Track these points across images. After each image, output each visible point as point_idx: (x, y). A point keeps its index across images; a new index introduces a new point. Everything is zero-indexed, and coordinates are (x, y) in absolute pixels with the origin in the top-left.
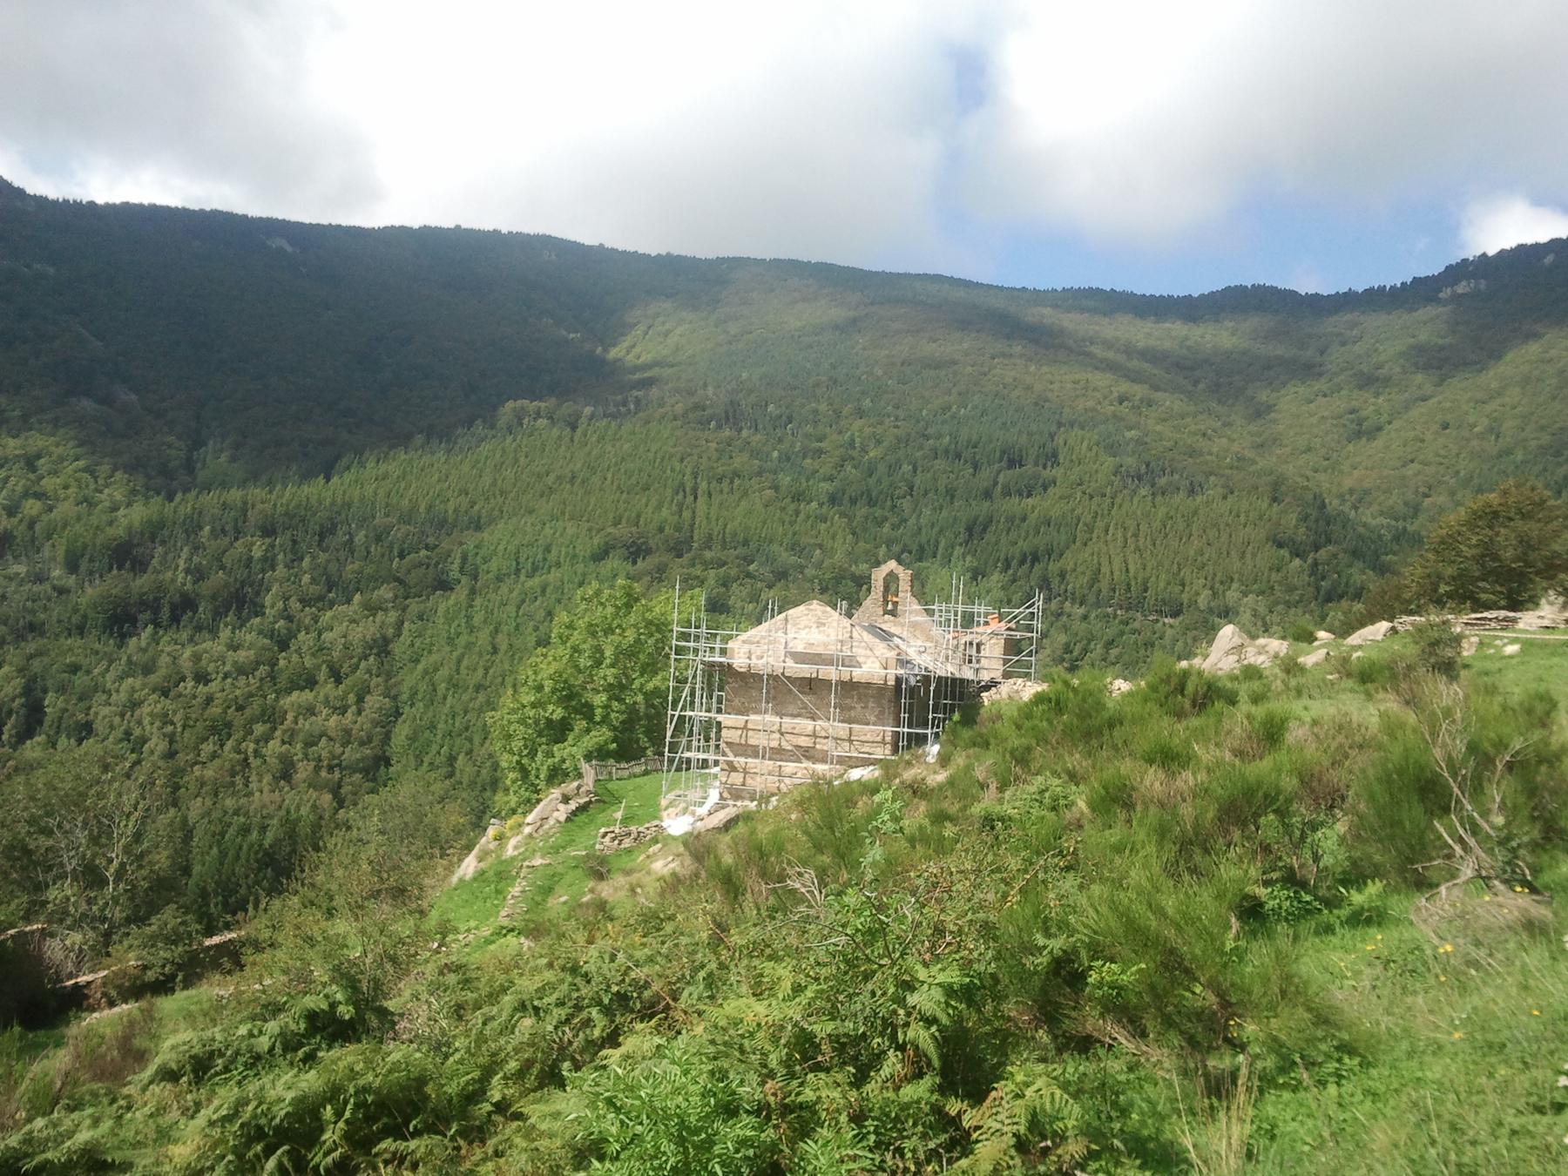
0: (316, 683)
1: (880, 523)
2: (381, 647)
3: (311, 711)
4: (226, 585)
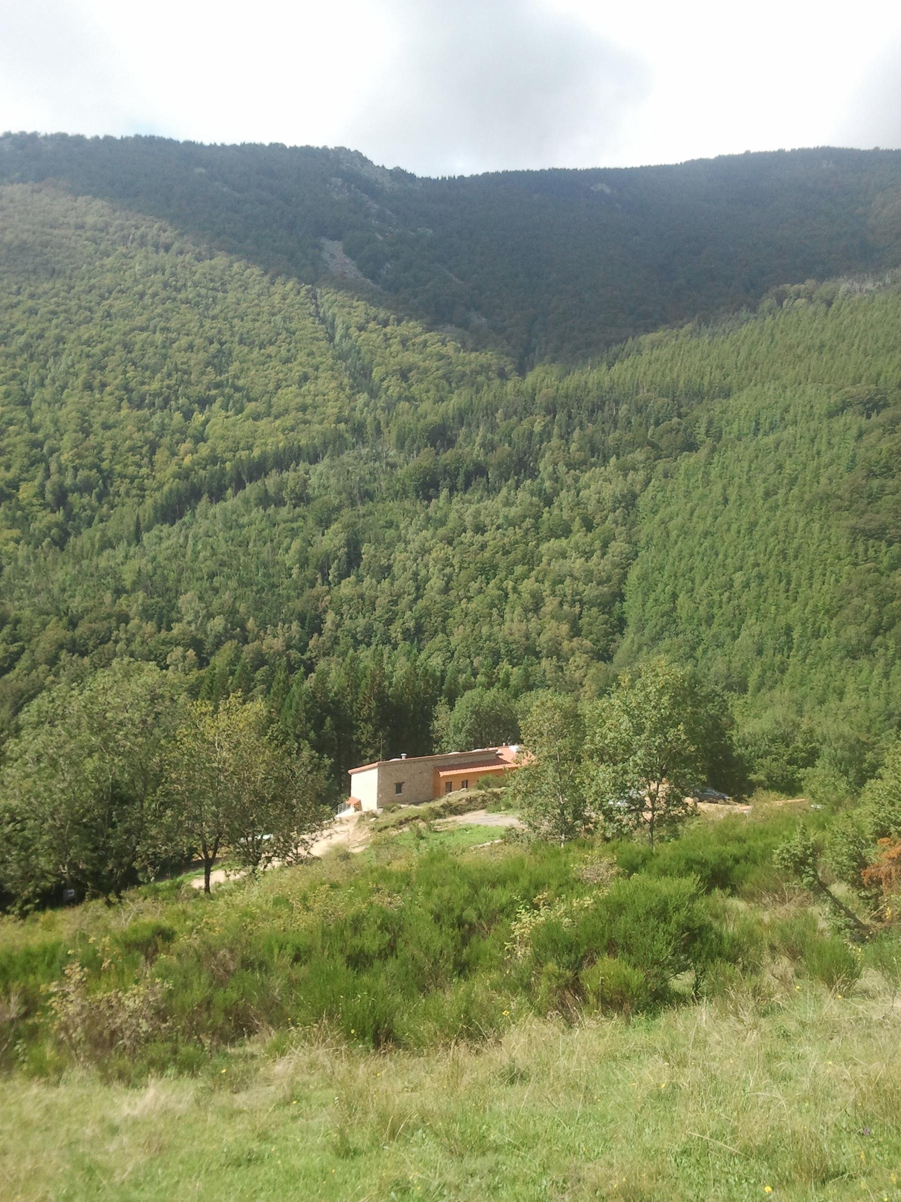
0: (571, 531)
2: (629, 501)
3: (563, 555)
4: (510, 455)
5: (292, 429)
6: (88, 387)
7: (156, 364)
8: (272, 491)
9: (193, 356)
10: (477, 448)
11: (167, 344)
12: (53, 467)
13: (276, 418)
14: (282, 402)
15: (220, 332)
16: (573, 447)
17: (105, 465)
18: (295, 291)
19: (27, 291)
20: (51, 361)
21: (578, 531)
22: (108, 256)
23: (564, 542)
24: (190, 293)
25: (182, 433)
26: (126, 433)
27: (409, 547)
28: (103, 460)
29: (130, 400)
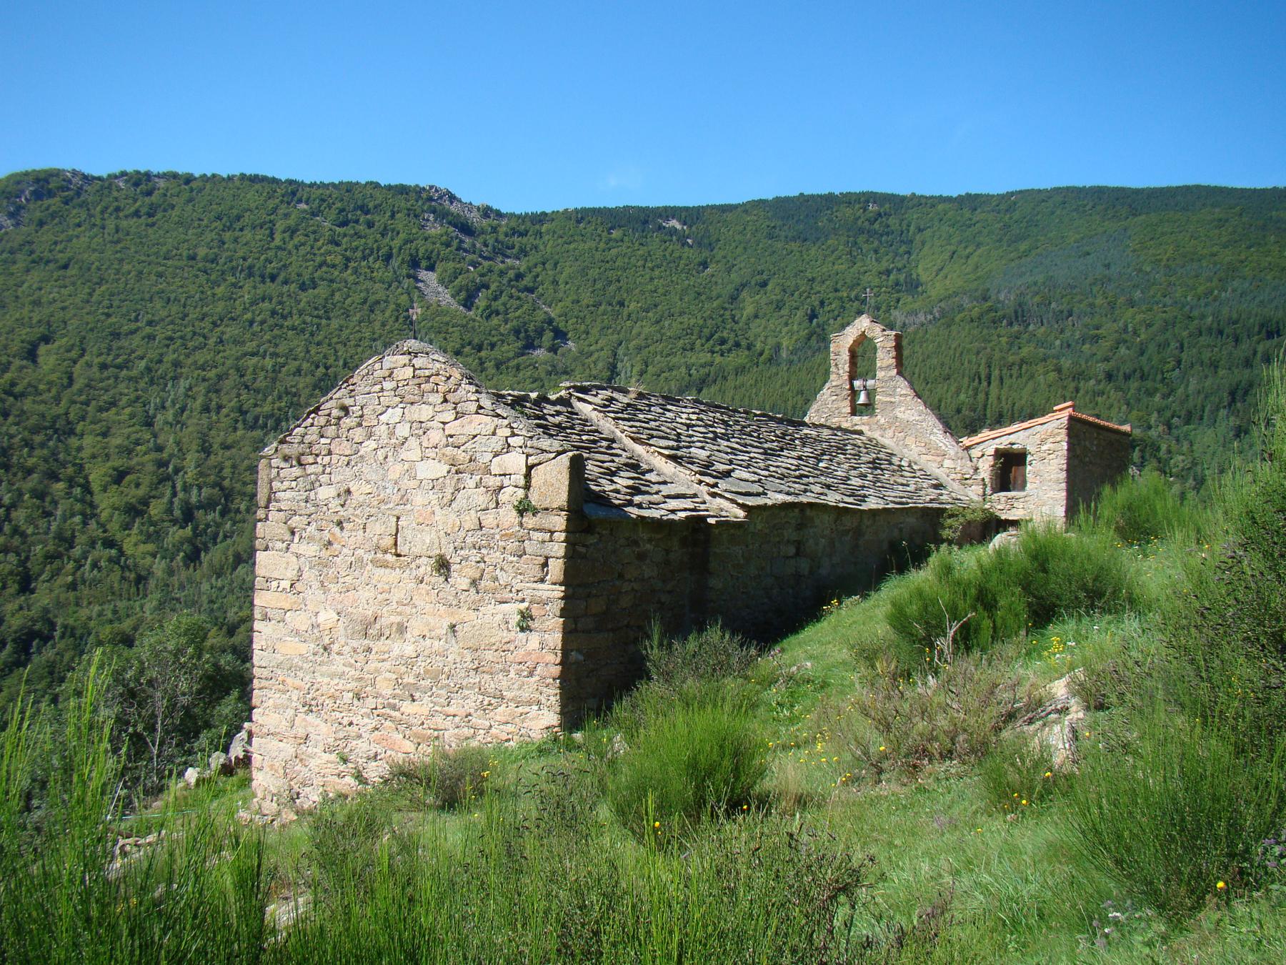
1: (1150, 393)
6: (206, 409)
11: (277, 368)
12: (179, 486)
15: (325, 357)
17: (226, 483)
18: (393, 318)
20: (170, 385)
22: (219, 286)
24: (296, 320)
26: (243, 453)
28: (224, 479)
29: (244, 421)
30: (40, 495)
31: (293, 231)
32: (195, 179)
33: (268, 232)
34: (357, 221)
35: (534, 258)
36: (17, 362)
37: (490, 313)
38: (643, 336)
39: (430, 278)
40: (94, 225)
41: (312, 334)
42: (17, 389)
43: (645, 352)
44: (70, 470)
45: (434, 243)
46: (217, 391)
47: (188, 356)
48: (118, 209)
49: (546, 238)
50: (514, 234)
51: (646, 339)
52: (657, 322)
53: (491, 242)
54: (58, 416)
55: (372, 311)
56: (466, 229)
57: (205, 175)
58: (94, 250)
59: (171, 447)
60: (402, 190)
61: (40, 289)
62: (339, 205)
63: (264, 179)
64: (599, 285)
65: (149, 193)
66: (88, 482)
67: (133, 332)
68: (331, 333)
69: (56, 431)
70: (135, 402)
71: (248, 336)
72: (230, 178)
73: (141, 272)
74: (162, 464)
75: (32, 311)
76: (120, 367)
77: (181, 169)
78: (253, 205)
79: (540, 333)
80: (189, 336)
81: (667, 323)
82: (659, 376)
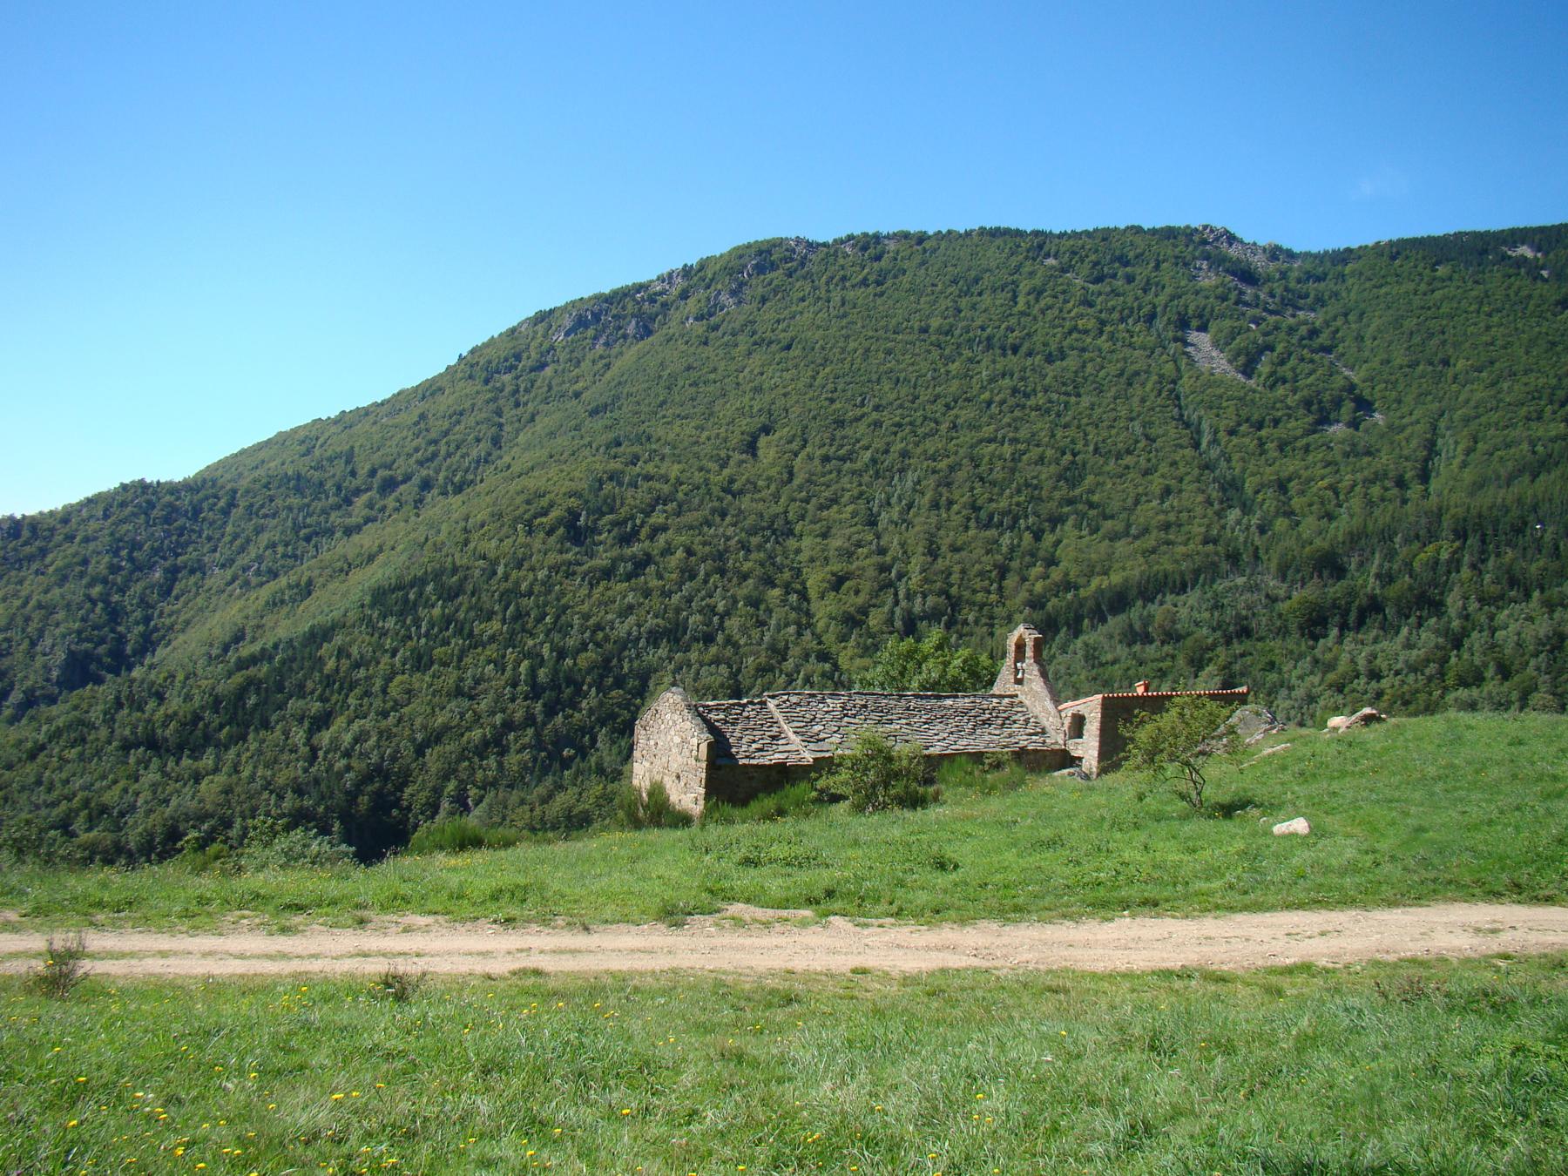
4: (1411, 588)
5: (1153, 551)
6: (935, 505)
7: (1004, 479)
8: (1137, 626)
9: (1045, 469)
10: (1372, 580)
12: (901, 595)
13: (1136, 537)
14: (1142, 520)
15: (1073, 442)
16: (1487, 578)
17: (954, 590)
18: (1155, 393)
19: (872, 403)
20: (896, 478)
21: (1492, 679)
22: (953, 362)
23: (1475, 692)
24: (1040, 399)
25: (1033, 555)
26: (974, 556)
27: (1293, 694)
28: (952, 585)
29: (978, 520)
30: (754, 603)
31: (1038, 293)
32: (929, 237)
33: (1010, 295)
34: (1114, 276)
35: (1333, 308)
36: (737, 456)
37: (1275, 381)
38: (1472, 403)
39: (1202, 341)
40: (819, 298)
41: (1058, 415)
42: (736, 487)
43: (1474, 425)
44: (787, 575)
45: (1207, 297)
46: (949, 485)
47: (917, 444)
48: (844, 279)
49: (1351, 281)
50: (1308, 279)
51: (1476, 407)
52: (1493, 384)
53: (1278, 291)
54: (776, 516)
55: (1130, 384)
56: (1248, 276)
57: (940, 232)
58: (819, 327)
59: (895, 549)
60: (1170, 233)
61: (762, 374)
62: (1093, 257)
63: (1006, 232)
64: (1417, 339)
65: (878, 258)
66: (805, 588)
67: (858, 419)
68: (1080, 414)
69: (774, 532)
70: (858, 498)
71: (984, 419)
72: (968, 234)
73: (868, 350)
74: (884, 568)
75: (753, 399)
76: (843, 459)
77: (913, 228)
78: (993, 265)
79: (1338, 403)
80: (919, 422)
81: (1505, 386)
82: (1492, 454)
